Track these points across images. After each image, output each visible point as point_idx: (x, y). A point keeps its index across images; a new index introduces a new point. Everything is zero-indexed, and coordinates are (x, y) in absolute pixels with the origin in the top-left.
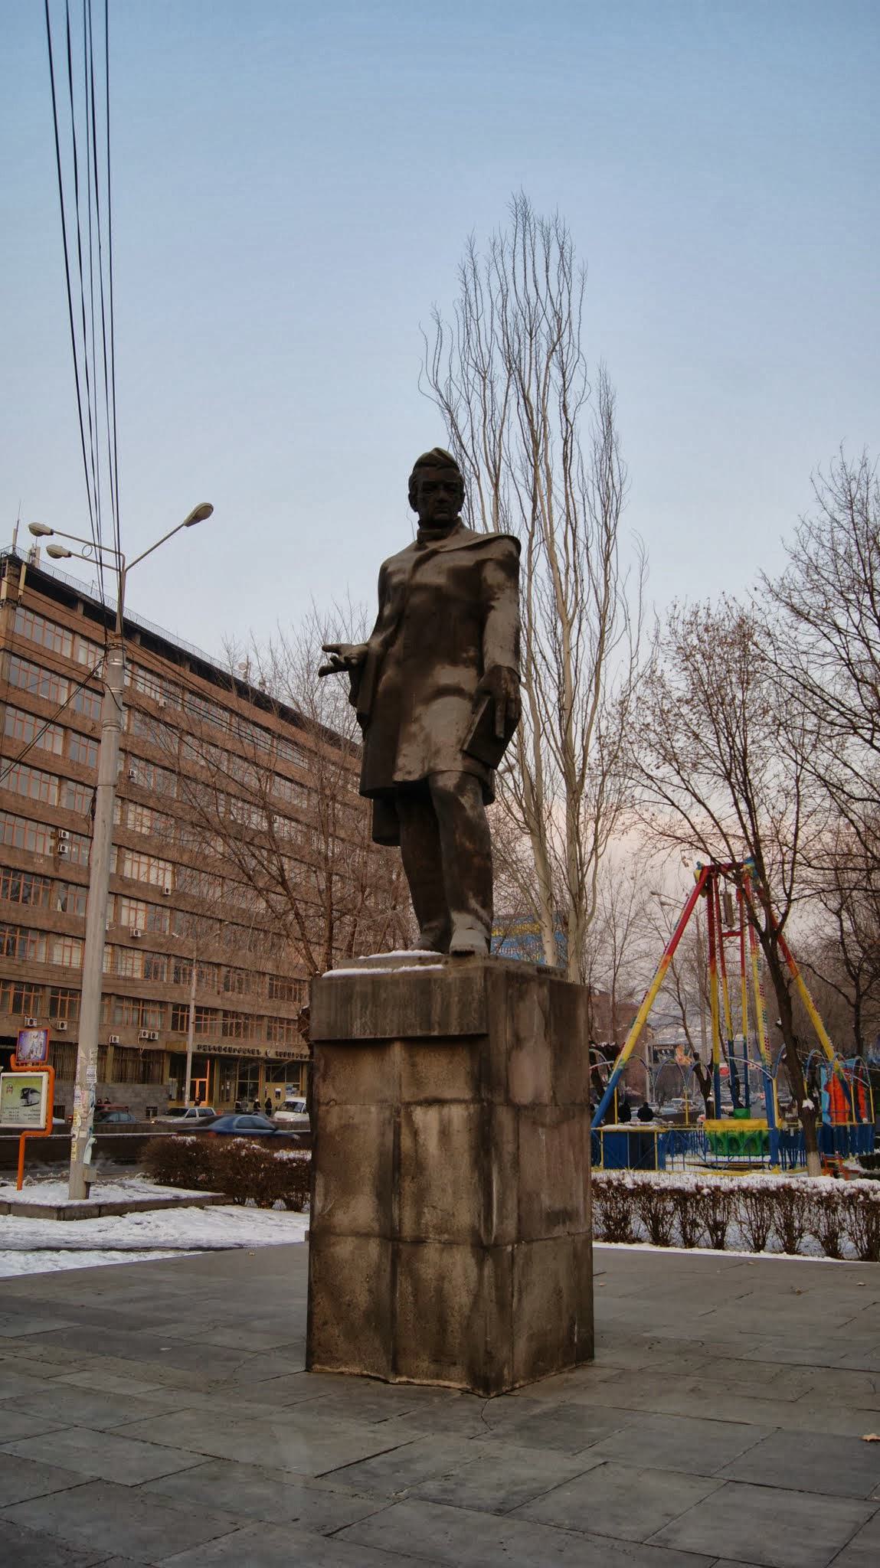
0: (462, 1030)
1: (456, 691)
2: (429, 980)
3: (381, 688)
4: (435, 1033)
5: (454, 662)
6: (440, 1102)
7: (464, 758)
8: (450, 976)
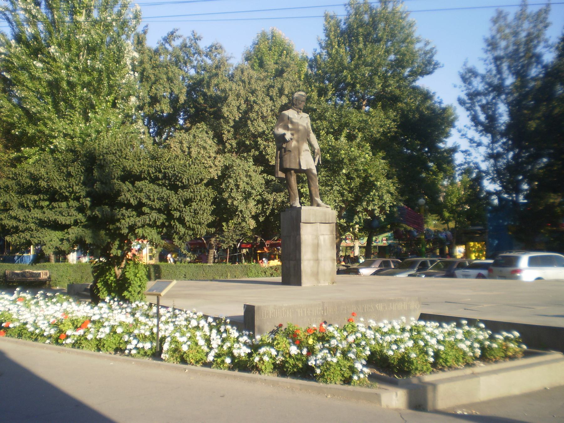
1: (308, 151)
6: (323, 235)
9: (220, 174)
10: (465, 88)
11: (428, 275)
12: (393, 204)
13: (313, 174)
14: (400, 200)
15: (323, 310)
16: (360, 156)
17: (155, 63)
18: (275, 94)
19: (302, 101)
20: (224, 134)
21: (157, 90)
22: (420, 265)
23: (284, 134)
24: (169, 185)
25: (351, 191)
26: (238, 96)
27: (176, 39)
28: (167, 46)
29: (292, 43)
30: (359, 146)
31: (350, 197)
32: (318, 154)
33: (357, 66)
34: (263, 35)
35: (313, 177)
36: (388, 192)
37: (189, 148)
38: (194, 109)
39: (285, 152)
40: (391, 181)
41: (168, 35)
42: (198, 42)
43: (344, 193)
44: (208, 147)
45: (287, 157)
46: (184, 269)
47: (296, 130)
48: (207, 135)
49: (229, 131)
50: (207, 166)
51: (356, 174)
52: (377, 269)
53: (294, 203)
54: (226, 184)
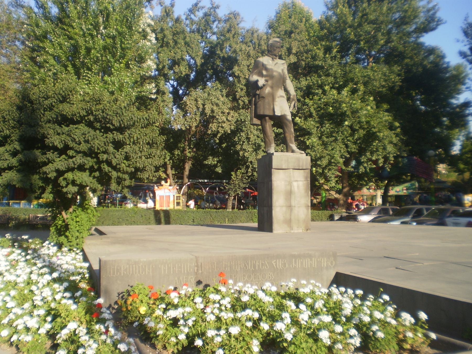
1: (284, 97)
6: (297, 181)
9: (233, 127)
10: (467, 43)
11: (419, 223)
12: (397, 154)
13: (287, 120)
14: (404, 151)
15: (197, 266)
16: (361, 109)
17: (176, 30)
18: (283, 54)
19: (277, 48)
20: (237, 92)
21: (175, 54)
22: (415, 213)
23: (257, 81)
24: (102, 128)
25: (355, 143)
26: (249, 56)
27: (200, 10)
28: (192, 16)
29: (311, 11)
30: (363, 100)
31: (354, 148)
32: (293, 100)
33: (360, 25)
34: (285, 6)
35: (288, 123)
36: (391, 142)
37: (204, 105)
38: (212, 71)
39: (259, 98)
40: (393, 132)
41: (193, 6)
42: (217, 10)
43: (347, 144)
44: (220, 104)
45: (260, 103)
46: (192, 214)
47: (270, 76)
48: (220, 93)
49: (242, 89)
50: (220, 121)
51: (358, 126)
52: (375, 216)
53: (268, 150)
54: (238, 137)
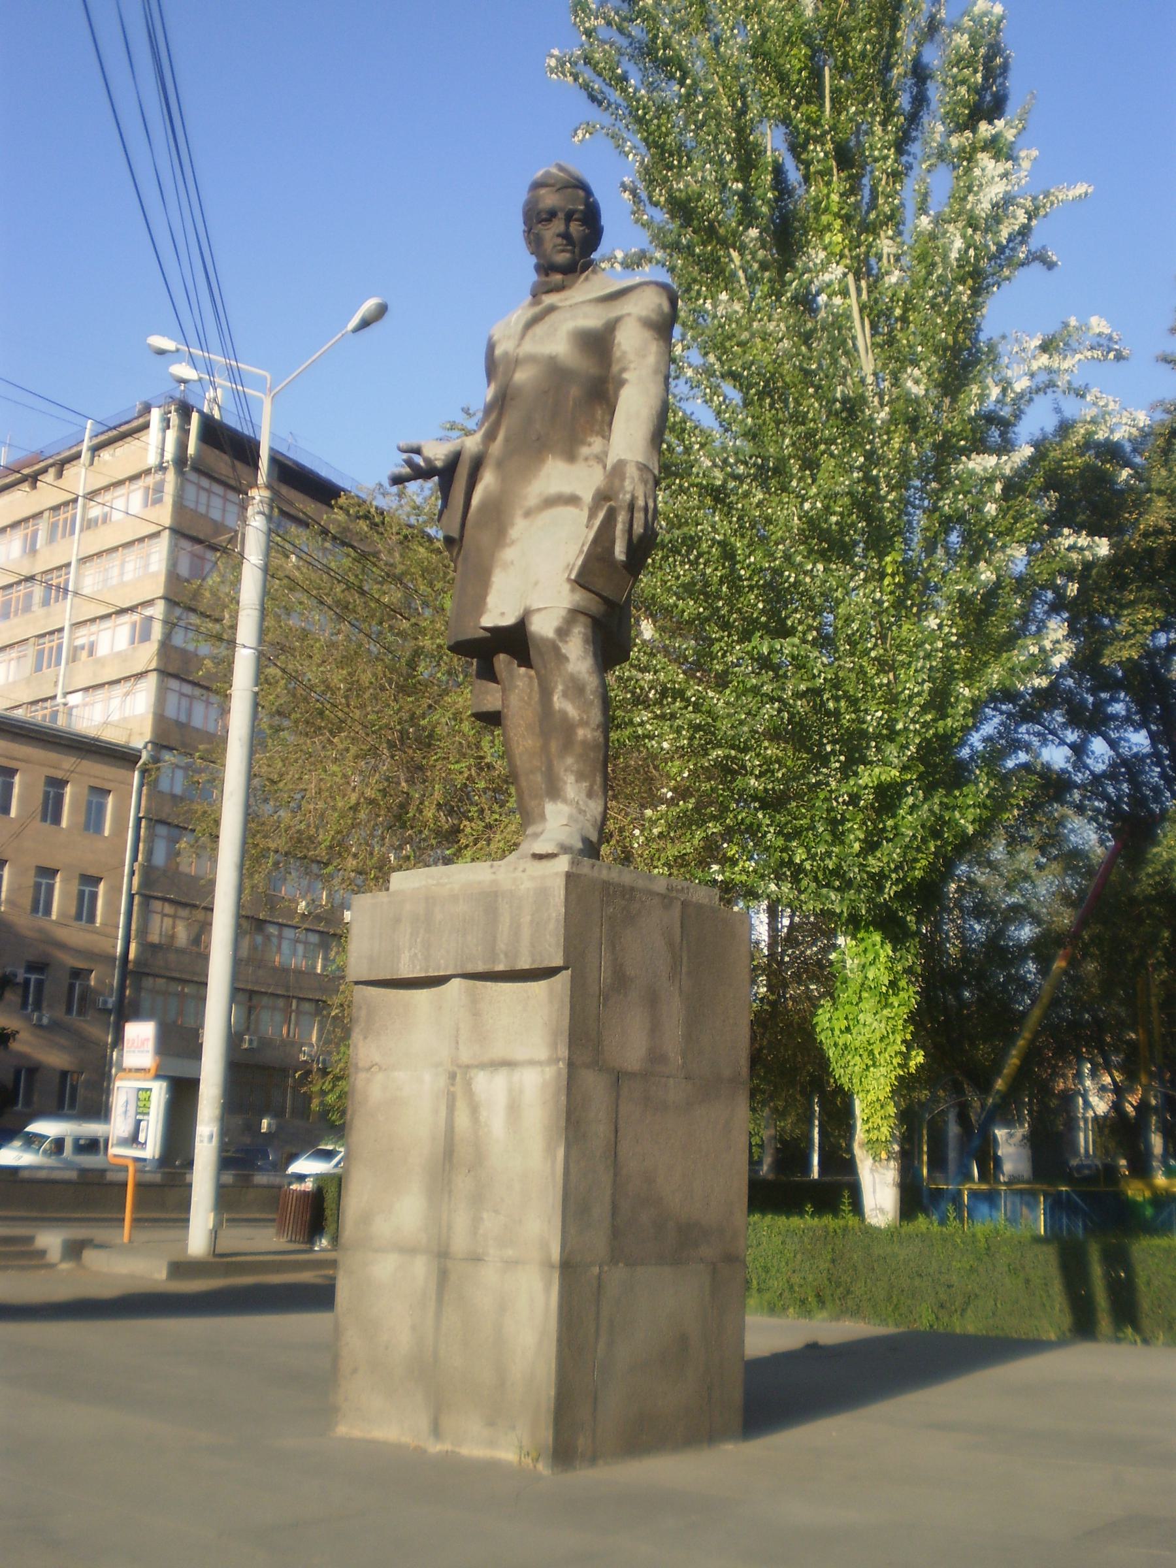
0: (534, 961)
1: (572, 500)
2: (495, 894)
3: (475, 501)
4: (500, 967)
5: (571, 456)
6: (509, 1064)
7: (573, 590)
8: (522, 887)
